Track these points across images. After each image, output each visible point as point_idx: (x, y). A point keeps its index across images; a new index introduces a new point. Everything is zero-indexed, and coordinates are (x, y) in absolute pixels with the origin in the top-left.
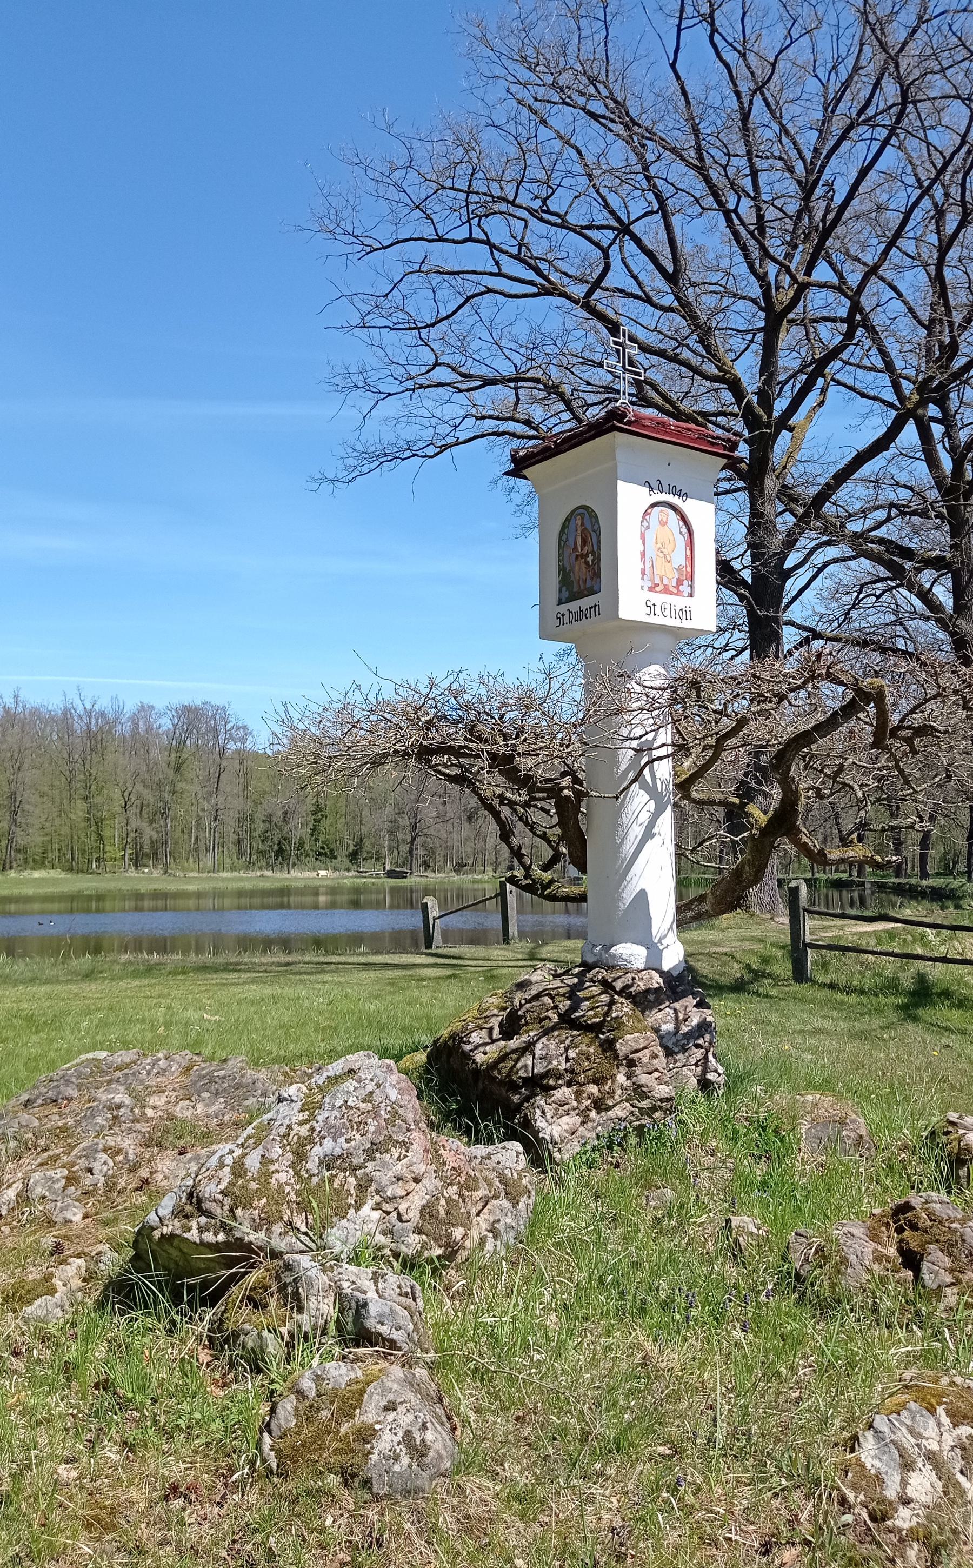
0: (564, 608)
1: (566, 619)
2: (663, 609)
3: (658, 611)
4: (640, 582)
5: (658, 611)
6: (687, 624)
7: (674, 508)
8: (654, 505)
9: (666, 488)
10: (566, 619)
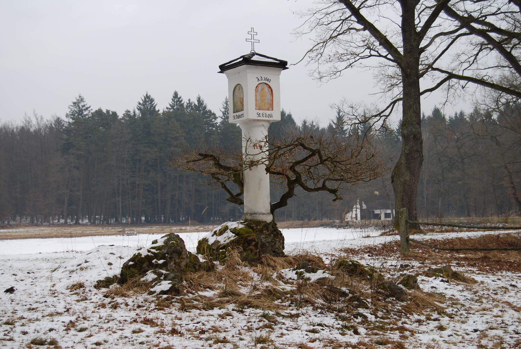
0: (235, 114)
2: (263, 115)
4: (254, 107)
5: (261, 115)
7: (267, 84)
9: (263, 79)
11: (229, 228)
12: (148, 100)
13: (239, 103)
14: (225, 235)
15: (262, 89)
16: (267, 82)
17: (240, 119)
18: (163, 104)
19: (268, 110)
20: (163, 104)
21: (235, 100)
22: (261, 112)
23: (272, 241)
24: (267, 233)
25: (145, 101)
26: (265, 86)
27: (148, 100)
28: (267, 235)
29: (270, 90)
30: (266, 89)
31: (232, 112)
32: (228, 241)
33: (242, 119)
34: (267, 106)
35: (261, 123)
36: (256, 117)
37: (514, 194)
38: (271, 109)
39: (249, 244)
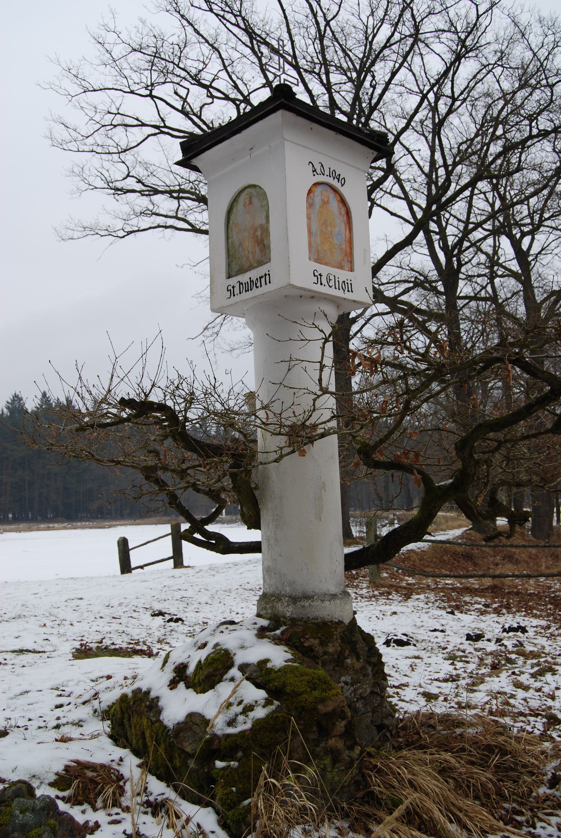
0: (234, 281)
1: (237, 291)
3: (324, 281)
5: (324, 281)
6: (348, 296)
8: (317, 184)
9: (327, 173)
10: (237, 291)
11: (240, 658)
12: (17, 399)
13: (249, 245)
14: (224, 689)
15: (325, 203)
16: (335, 183)
17: (256, 292)
18: (31, 404)
19: (341, 267)
20: (31, 404)
21: (235, 238)
22: (324, 270)
23: (372, 693)
24: (358, 665)
25: (13, 400)
26: (331, 195)
27: (17, 399)
28: (356, 672)
29: (343, 211)
30: (334, 204)
31: (224, 275)
32: (244, 725)
33: (265, 289)
34: (338, 257)
35: (316, 306)
36: (309, 283)
37: (376, 490)
38: (347, 265)
39: (324, 732)
